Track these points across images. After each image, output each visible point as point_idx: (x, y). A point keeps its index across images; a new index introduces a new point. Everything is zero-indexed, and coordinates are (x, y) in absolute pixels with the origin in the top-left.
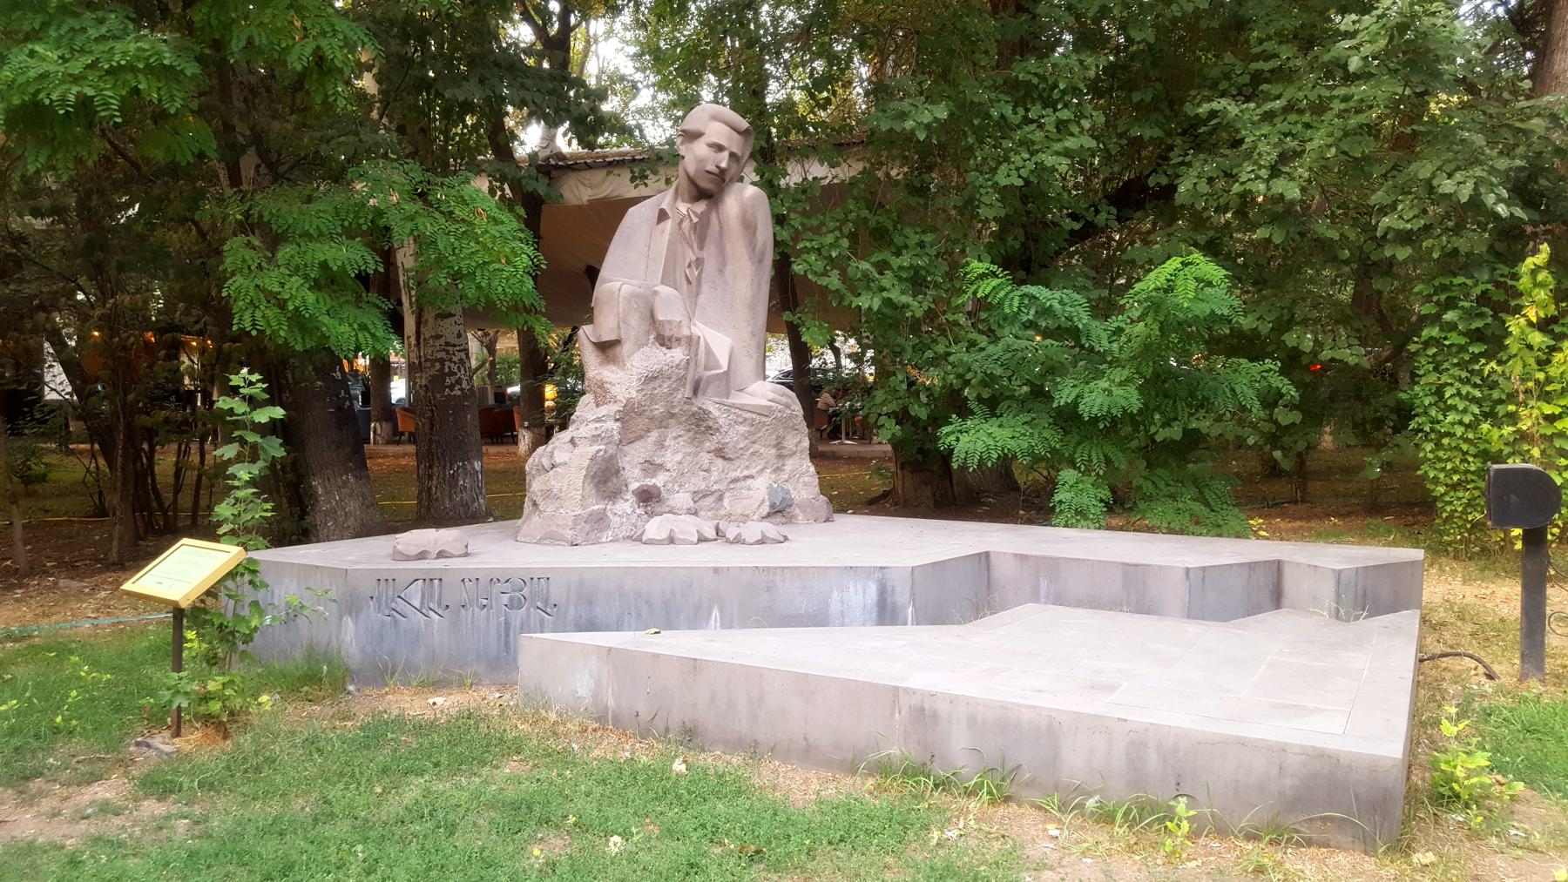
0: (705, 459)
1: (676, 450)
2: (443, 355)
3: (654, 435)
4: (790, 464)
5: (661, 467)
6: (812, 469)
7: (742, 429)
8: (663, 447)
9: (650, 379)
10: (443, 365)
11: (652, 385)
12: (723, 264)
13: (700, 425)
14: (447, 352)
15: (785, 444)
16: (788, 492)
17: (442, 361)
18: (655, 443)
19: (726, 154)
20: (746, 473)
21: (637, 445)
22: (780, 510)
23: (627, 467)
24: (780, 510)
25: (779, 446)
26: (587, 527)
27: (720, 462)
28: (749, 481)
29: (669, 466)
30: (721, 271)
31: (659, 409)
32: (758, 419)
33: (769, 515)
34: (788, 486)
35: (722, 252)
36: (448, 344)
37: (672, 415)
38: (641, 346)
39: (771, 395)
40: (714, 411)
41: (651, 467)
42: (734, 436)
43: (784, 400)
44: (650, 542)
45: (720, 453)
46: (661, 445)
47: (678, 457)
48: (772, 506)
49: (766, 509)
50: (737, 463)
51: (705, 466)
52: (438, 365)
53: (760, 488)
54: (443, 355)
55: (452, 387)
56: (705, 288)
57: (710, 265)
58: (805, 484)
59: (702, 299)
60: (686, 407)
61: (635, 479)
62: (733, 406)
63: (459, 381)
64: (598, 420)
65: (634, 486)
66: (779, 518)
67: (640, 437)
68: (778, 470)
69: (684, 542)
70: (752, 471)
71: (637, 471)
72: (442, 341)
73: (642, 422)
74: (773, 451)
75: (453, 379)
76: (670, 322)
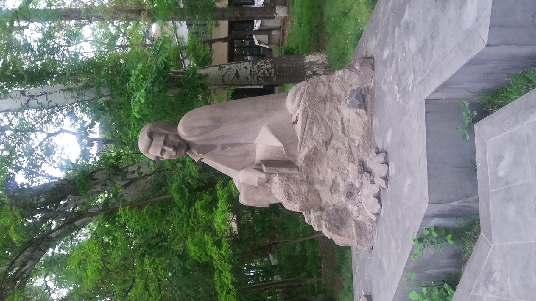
0: (331, 152)
1: (325, 172)
2: (256, 77)
3: (317, 187)
4: (337, 90)
5: (334, 181)
6: (340, 72)
7: (315, 130)
8: (324, 181)
9: (289, 197)
10: (260, 77)
11: (292, 195)
12: (223, 137)
13: (313, 158)
14: (254, 75)
15: (324, 95)
16: (353, 91)
17: (258, 77)
18: (321, 186)
19: (166, 148)
20: (339, 123)
21: (322, 196)
22: (363, 99)
23: (333, 202)
24: (363, 99)
25: (324, 101)
26: (364, 238)
27: (333, 142)
28: (345, 120)
29: (334, 177)
30: (227, 137)
31: (304, 188)
32: (312, 118)
33: (365, 109)
34: (349, 90)
35: (217, 138)
36: (250, 74)
37: (308, 177)
38: (271, 192)
39: (295, 105)
40: (305, 151)
41: (334, 188)
42: (319, 135)
43: (298, 98)
44: (377, 221)
45: (327, 143)
46: (322, 182)
47: (329, 170)
48: (360, 107)
49: (362, 111)
50: (334, 130)
51: (334, 152)
52: (260, 79)
53: (350, 114)
54: (256, 77)
55: (270, 73)
56: (236, 141)
57: (225, 141)
58: (349, 78)
59: (242, 141)
60: (303, 171)
61: (339, 199)
62: (302, 138)
63: (267, 69)
64: (310, 221)
65: (343, 199)
66: (368, 99)
67: (319, 195)
68: (339, 100)
69: (380, 210)
70: (339, 119)
71: (336, 196)
72: (249, 77)
73: (312, 198)
74: (328, 104)
75: (266, 72)
76: (258, 182)
